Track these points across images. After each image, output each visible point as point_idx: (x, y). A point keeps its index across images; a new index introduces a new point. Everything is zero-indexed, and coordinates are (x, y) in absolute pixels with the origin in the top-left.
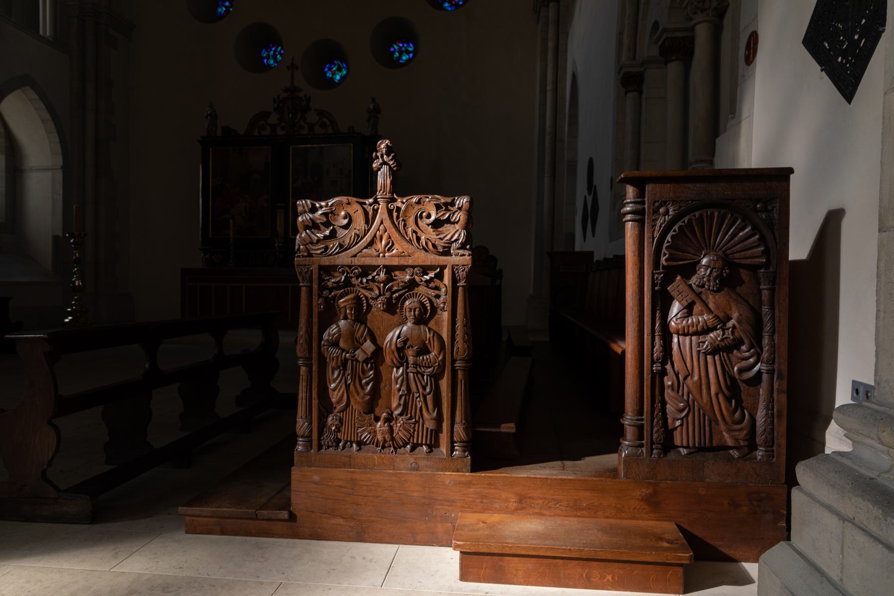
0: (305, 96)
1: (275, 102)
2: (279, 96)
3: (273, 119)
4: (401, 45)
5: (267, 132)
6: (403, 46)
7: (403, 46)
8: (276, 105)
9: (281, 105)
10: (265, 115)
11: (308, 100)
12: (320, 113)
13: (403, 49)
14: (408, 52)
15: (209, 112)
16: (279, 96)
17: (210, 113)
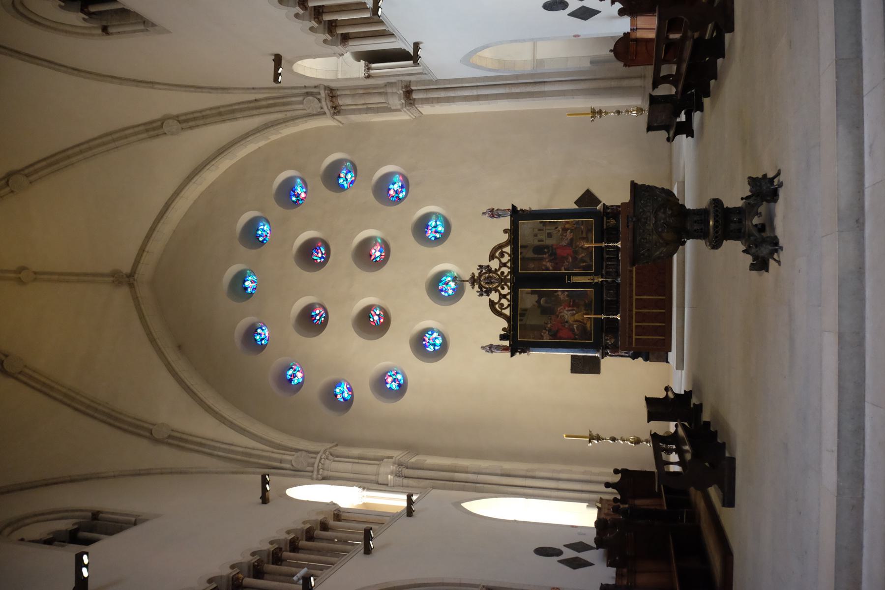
0: (478, 269)
1: (482, 295)
2: (477, 292)
3: (494, 296)
4: (430, 232)
5: (505, 302)
6: (431, 229)
7: (431, 229)
8: (485, 294)
9: (484, 290)
10: (492, 304)
11: (481, 266)
12: (492, 257)
13: (433, 230)
14: (436, 226)
15: (488, 349)
16: (477, 292)
17: (489, 347)
